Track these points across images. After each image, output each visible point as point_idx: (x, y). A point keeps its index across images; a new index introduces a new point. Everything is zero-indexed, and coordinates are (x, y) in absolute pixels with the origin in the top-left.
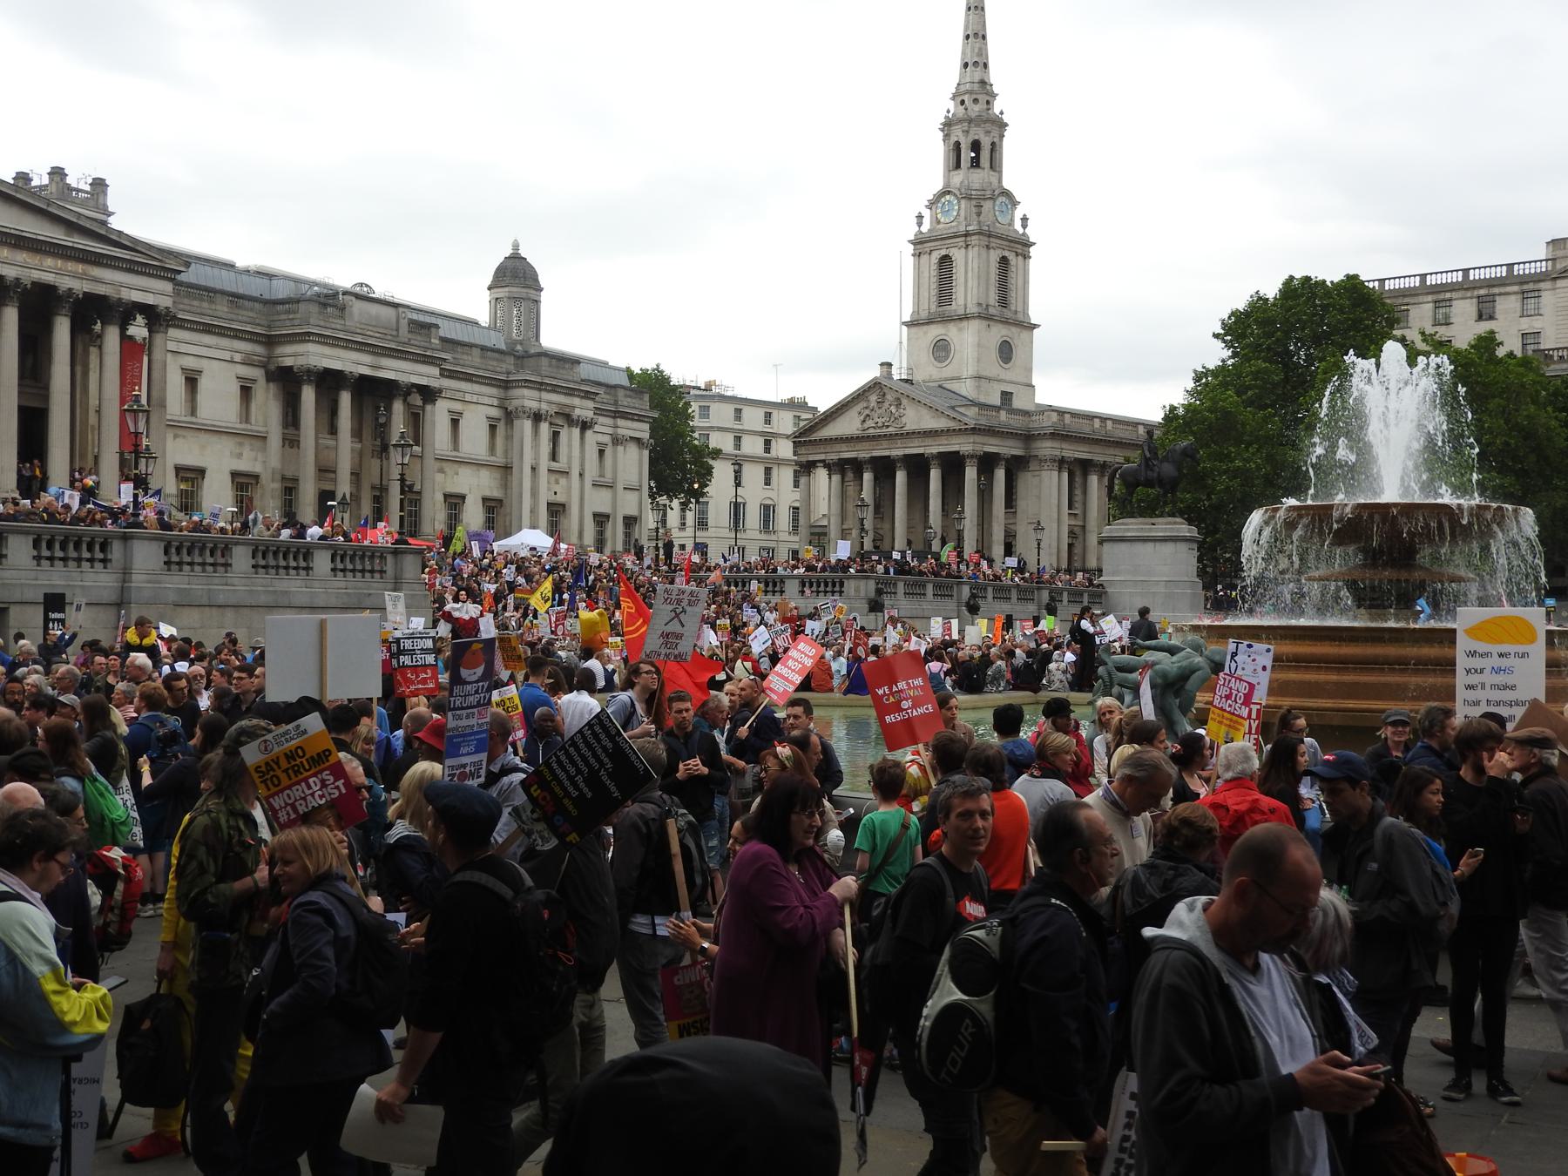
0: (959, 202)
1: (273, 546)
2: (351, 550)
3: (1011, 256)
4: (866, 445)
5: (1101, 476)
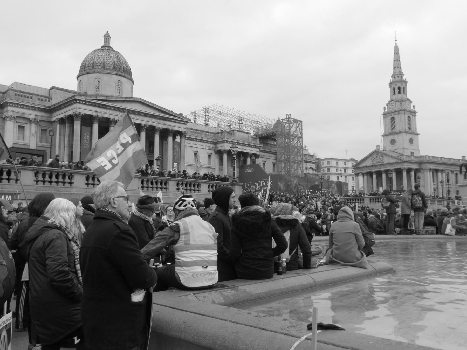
0: (395, 103)
2: (215, 184)
3: (411, 116)
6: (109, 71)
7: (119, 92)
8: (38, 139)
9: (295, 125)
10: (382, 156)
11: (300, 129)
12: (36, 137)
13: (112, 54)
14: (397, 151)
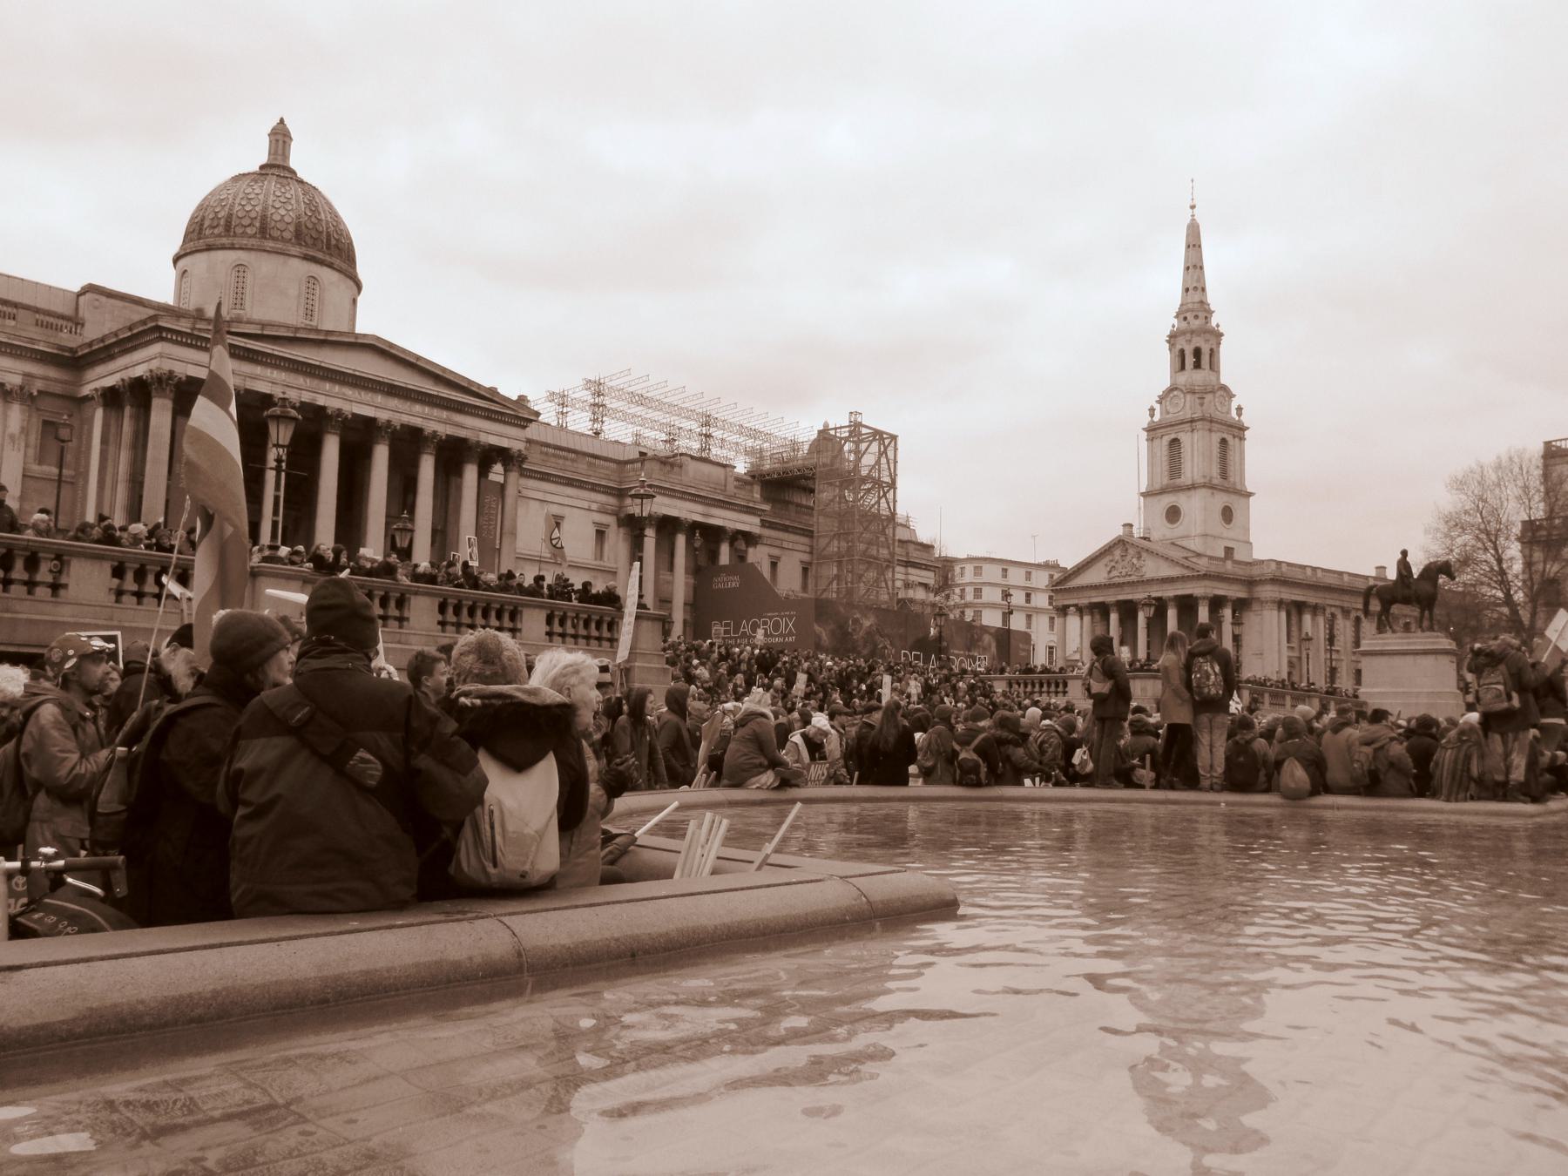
1: (467, 599)
2: (573, 611)
3: (1229, 438)
4: (1112, 591)
5: (1314, 614)
6: (279, 245)
7: (309, 313)
8: (31, 452)
9: (875, 447)
10: (1139, 558)
12: (23, 444)
13: (293, 192)
14: (1184, 543)
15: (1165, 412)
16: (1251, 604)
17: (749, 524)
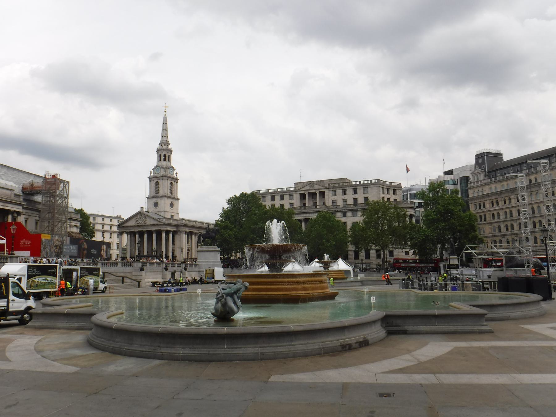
3: (173, 182)
5: (195, 236)
10: (145, 218)
11: (66, 189)
14: (159, 213)
15: (155, 173)
16: (177, 232)
17: (18, 209)
